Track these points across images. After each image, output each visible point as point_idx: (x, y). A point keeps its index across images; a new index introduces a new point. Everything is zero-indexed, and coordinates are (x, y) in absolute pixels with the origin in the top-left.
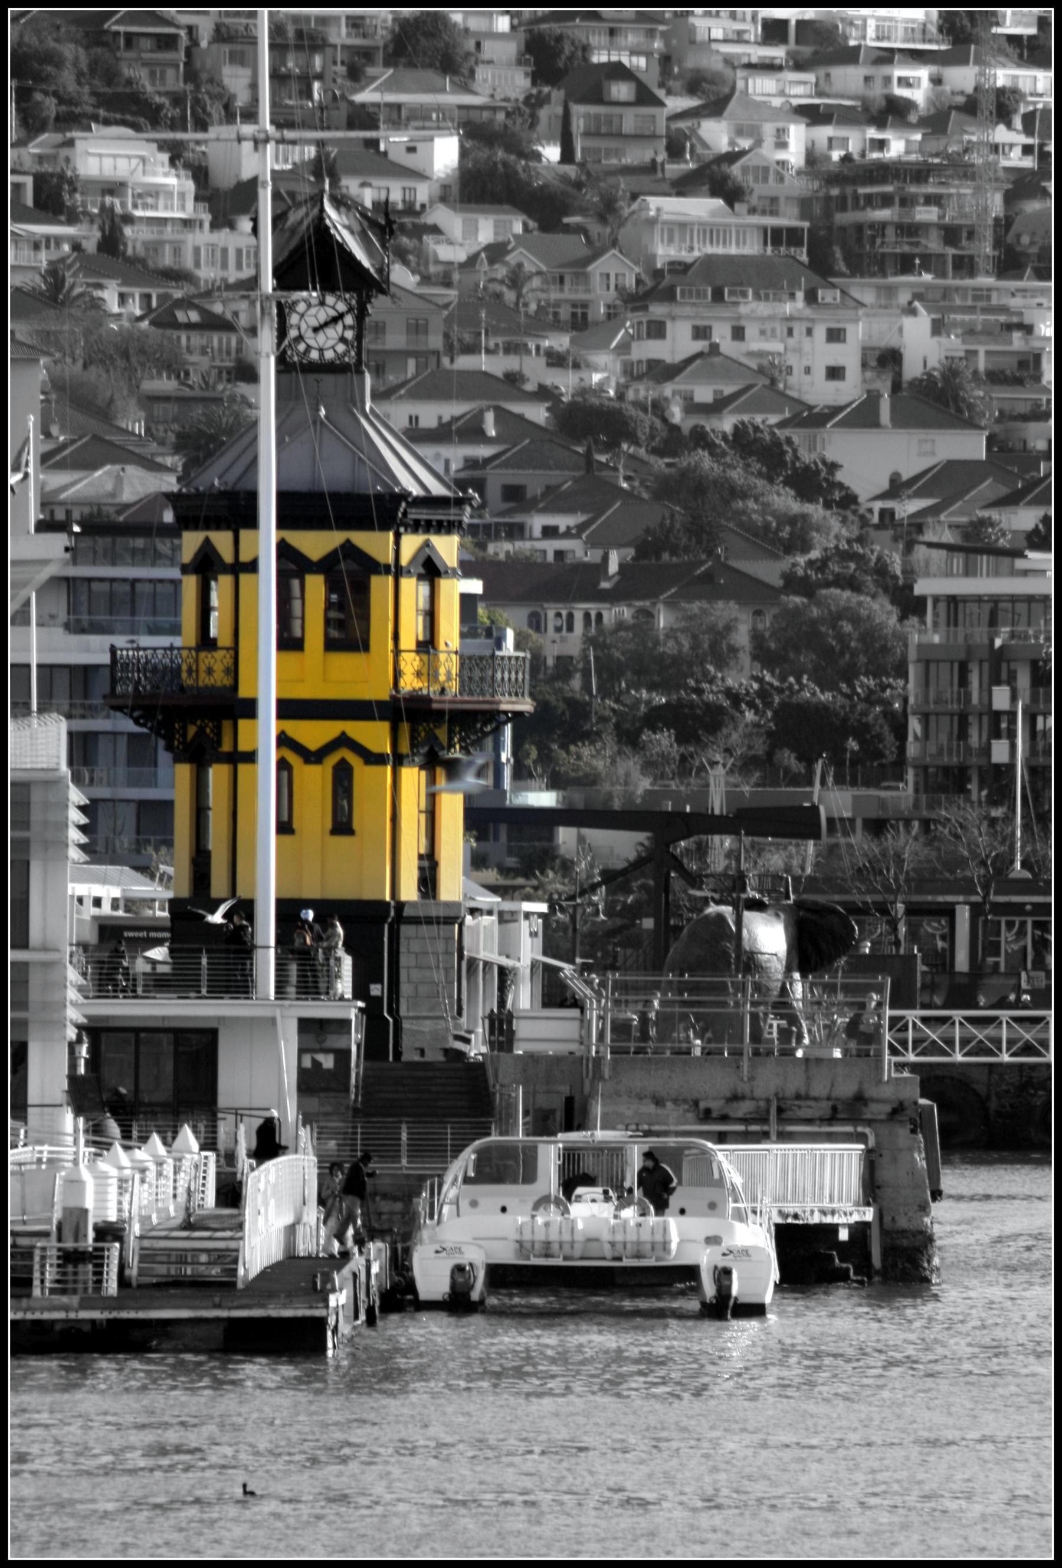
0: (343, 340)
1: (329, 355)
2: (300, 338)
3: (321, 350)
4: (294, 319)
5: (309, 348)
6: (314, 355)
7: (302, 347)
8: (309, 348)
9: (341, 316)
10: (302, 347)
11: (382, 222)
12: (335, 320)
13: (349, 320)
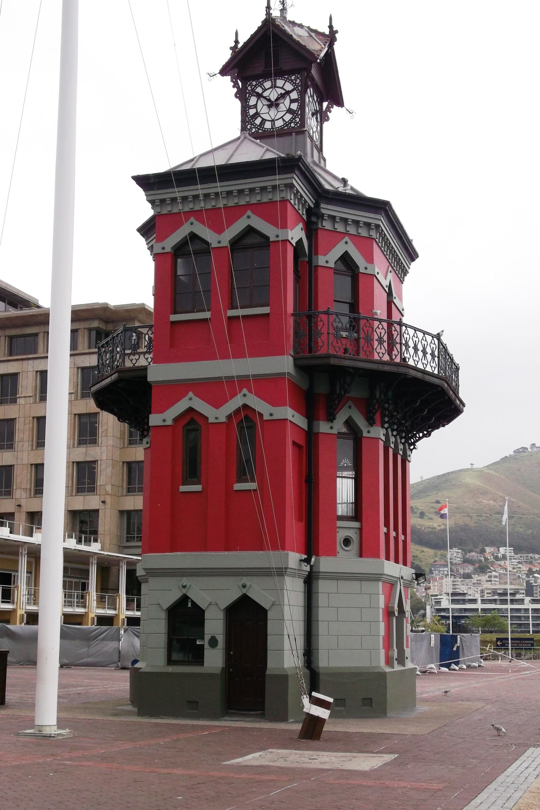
0: (289, 111)
1: (279, 124)
2: (257, 115)
3: (273, 121)
4: (253, 101)
5: (264, 121)
6: (268, 125)
7: (258, 121)
8: (264, 121)
9: (288, 93)
10: (258, 121)
11: (327, 32)
12: (282, 96)
13: (294, 95)
